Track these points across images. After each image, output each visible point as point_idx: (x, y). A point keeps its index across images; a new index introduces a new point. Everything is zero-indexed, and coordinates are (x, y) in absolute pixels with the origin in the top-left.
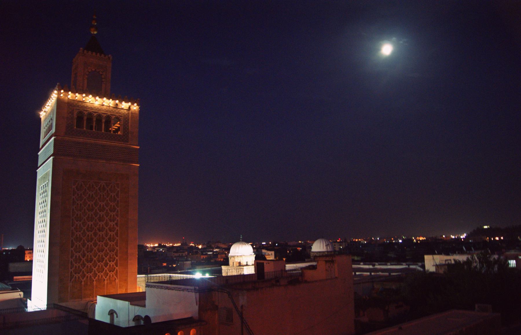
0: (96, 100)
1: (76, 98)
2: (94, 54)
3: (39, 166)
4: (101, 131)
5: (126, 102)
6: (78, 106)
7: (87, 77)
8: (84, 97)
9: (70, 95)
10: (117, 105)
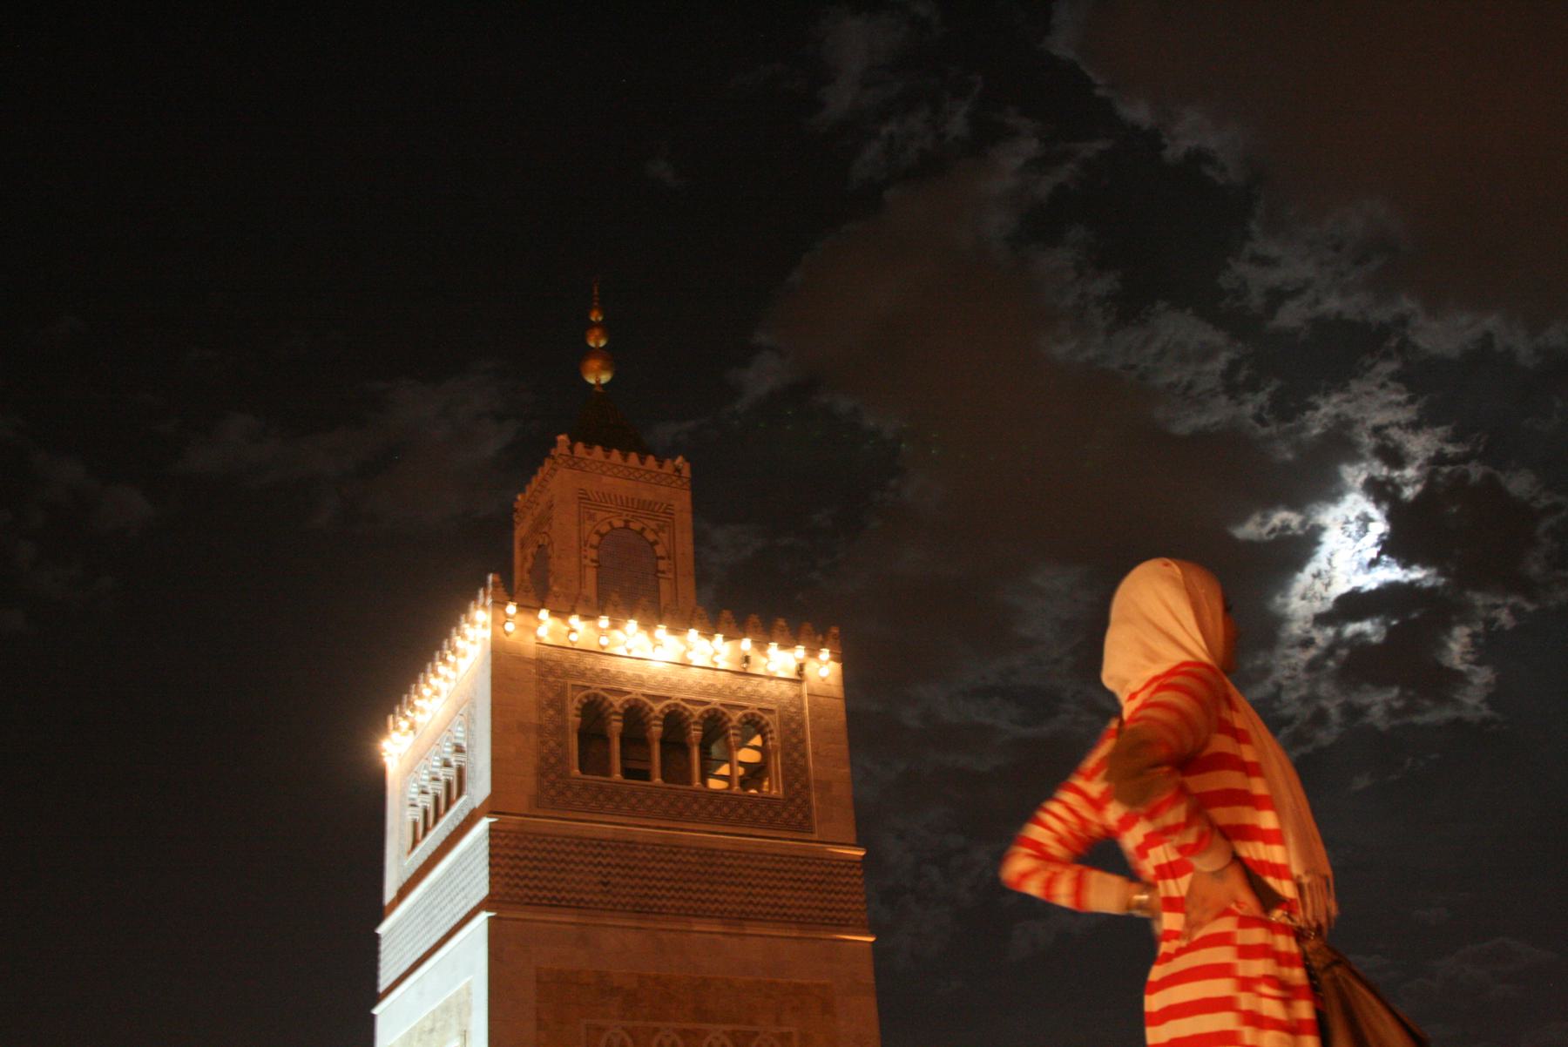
0: (657, 645)
1: (573, 637)
2: (616, 455)
3: (381, 989)
4: (689, 782)
5: (783, 646)
6: (582, 674)
7: (593, 554)
8: (601, 632)
9: (548, 628)
10: (747, 659)
